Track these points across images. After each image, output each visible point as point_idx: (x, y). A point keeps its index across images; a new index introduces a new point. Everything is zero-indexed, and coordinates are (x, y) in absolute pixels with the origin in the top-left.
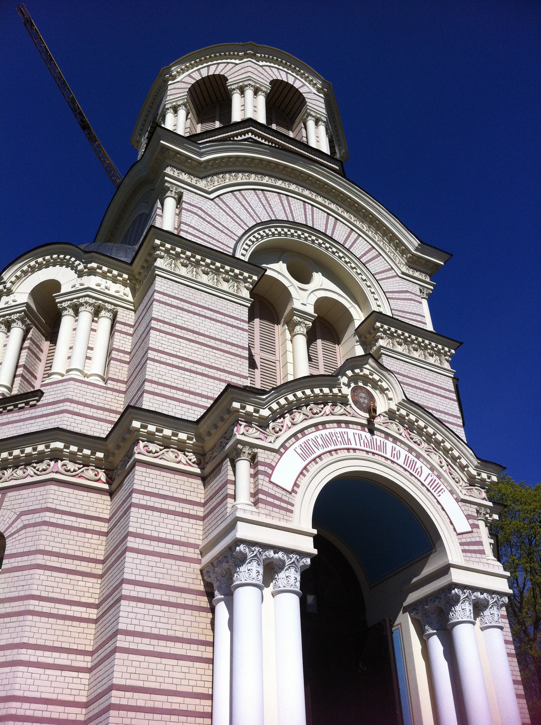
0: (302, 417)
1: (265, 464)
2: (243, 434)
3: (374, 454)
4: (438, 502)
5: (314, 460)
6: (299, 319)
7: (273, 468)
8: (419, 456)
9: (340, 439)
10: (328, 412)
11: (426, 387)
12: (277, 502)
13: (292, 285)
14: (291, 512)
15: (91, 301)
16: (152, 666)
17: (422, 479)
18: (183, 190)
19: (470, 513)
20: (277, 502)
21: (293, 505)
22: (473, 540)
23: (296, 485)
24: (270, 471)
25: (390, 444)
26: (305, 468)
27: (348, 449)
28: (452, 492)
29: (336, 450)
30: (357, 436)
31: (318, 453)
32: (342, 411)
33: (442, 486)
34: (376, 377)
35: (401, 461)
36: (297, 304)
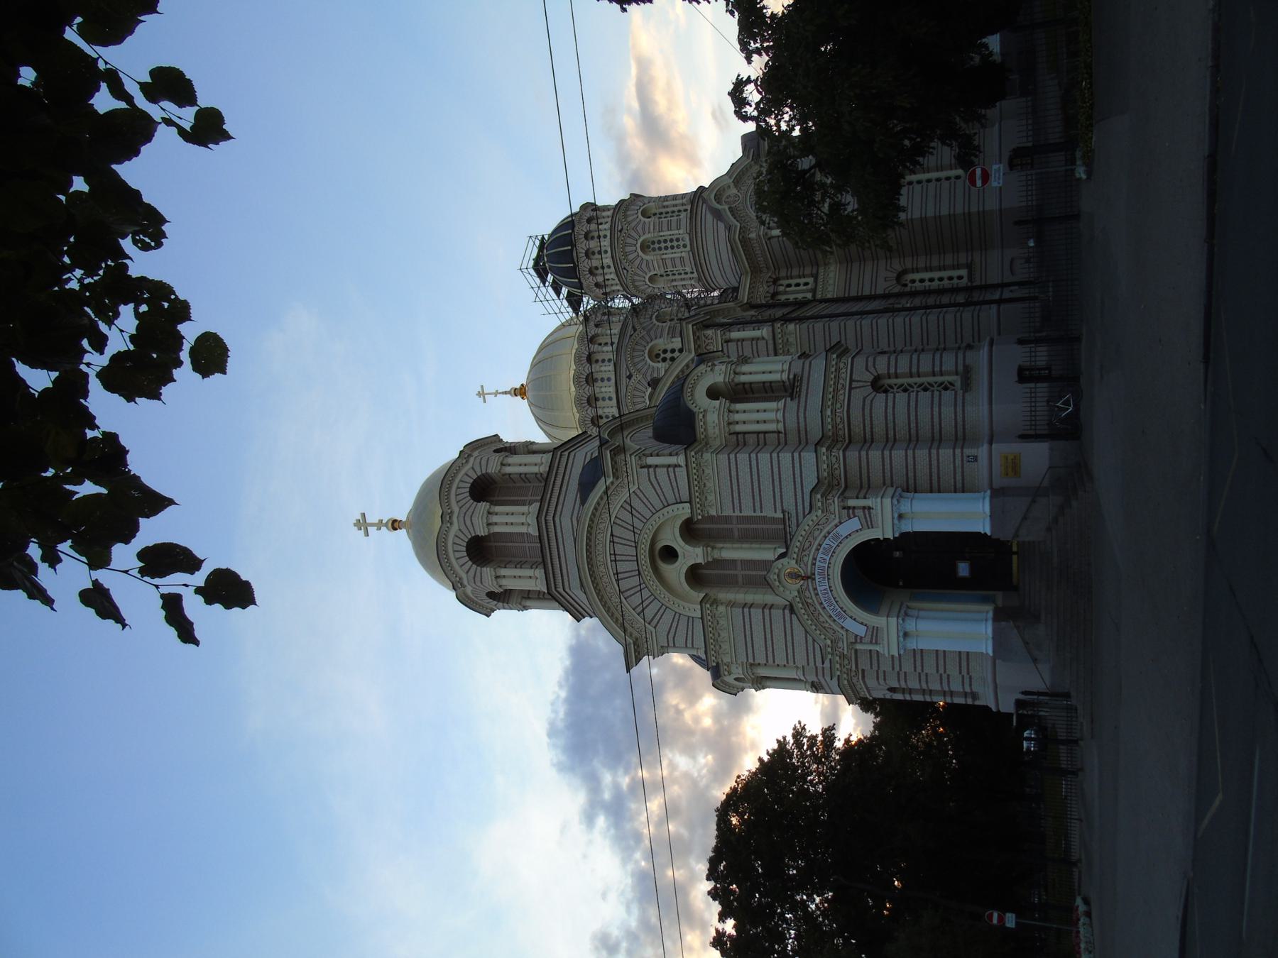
1: (856, 640)
2: (843, 649)
3: (828, 575)
4: (847, 537)
5: (844, 612)
7: (856, 636)
8: (820, 545)
9: (826, 595)
10: (811, 601)
11: (734, 481)
12: (875, 634)
18: (659, 647)
20: (875, 634)
21: (874, 627)
22: (863, 517)
23: (862, 624)
24: (859, 637)
25: (818, 564)
26: (851, 617)
27: (831, 591)
28: (837, 526)
29: (834, 598)
31: (839, 610)
32: (808, 592)
34: (777, 571)
36: (700, 560)
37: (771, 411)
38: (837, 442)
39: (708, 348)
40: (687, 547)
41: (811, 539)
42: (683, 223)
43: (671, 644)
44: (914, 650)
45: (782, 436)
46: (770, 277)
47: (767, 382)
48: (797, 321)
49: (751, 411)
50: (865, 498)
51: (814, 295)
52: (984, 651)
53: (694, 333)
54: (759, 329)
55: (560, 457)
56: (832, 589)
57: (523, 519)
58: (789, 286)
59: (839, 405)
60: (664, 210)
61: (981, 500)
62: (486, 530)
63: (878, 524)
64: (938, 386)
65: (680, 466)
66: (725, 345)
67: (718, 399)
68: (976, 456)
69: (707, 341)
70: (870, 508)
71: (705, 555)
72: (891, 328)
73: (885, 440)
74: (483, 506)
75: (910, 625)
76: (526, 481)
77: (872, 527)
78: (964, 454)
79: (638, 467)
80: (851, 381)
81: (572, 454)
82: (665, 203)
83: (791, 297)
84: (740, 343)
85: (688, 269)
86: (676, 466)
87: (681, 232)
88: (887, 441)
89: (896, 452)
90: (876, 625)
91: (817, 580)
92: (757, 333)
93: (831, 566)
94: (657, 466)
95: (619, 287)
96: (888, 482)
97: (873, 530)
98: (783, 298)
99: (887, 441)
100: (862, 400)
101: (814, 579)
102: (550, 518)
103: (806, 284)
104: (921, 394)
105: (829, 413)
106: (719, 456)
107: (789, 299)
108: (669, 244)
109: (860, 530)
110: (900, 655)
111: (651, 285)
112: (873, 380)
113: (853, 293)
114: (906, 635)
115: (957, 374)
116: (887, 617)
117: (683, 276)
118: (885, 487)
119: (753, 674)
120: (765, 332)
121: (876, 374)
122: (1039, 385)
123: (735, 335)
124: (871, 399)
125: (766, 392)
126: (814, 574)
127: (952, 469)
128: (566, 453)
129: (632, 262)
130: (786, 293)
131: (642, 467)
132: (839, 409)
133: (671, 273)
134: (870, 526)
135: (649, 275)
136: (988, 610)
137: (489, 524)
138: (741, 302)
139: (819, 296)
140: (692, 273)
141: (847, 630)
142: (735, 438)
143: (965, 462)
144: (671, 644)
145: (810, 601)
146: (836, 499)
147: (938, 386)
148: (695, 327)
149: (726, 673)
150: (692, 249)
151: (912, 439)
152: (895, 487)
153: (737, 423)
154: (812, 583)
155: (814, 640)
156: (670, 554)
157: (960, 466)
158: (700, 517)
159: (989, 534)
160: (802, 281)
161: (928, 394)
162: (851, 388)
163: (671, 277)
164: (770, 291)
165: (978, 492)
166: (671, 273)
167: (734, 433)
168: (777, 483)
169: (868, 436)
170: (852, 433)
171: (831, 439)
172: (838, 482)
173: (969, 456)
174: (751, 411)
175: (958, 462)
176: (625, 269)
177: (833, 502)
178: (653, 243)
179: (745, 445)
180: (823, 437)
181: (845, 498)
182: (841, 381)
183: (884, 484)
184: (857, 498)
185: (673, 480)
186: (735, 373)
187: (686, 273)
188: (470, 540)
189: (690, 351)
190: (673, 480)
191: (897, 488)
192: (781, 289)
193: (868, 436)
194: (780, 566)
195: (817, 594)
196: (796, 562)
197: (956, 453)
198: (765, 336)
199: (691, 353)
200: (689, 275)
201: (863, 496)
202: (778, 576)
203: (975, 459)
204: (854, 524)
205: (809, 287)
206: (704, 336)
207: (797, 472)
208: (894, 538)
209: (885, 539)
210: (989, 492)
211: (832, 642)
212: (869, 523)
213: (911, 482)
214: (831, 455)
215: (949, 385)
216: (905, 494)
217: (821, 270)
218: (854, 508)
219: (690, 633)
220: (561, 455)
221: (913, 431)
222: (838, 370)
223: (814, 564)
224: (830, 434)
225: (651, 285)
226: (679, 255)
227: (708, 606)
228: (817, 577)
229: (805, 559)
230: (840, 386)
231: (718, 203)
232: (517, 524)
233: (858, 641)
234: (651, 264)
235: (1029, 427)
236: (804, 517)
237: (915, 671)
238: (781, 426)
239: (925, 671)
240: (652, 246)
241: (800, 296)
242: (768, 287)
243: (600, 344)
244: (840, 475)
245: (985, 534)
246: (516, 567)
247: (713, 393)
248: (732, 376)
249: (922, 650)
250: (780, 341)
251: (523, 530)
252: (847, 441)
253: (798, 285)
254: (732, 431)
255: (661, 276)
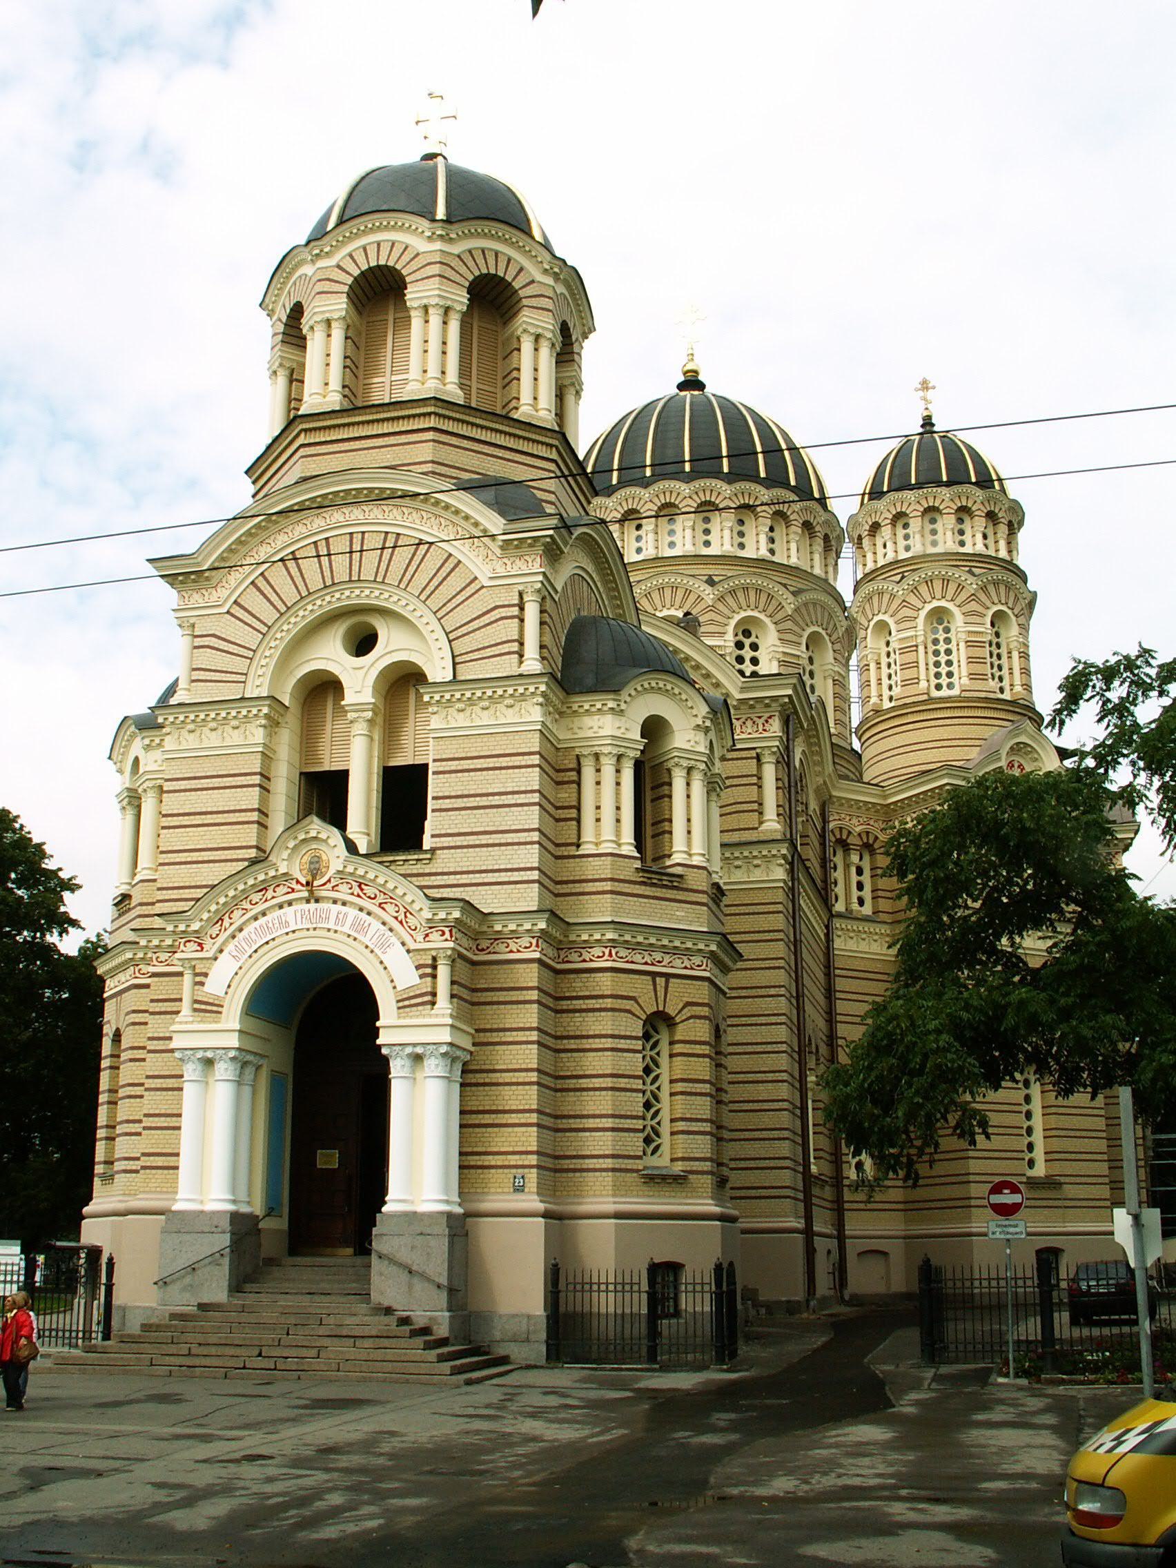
0: (241, 912)
4: (381, 962)
6: (354, 715)
7: (206, 975)
13: (345, 669)
14: (220, 1013)
15: (149, 784)
16: (167, 1137)
17: (366, 941)
19: (421, 962)
20: (209, 1008)
21: (222, 1006)
27: (287, 934)
28: (403, 944)
30: (299, 915)
33: (394, 940)
34: (323, 836)
35: (346, 929)
36: (350, 698)
37: (618, 833)
38: (558, 949)
39: (749, 723)
40: (374, 673)
41: (381, 898)
42: (979, 685)
43: (198, 642)
44: (182, 1076)
45: (572, 851)
46: (876, 838)
47: (671, 827)
48: (790, 884)
49: (618, 794)
50: (452, 996)
51: (840, 915)
52: (178, 1197)
53: (774, 699)
54: (778, 815)
55: (547, 445)
56: (291, 934)
57: (433, 371)
58: (860, 871)
59: (623, 953)
60: (1004, 651)
61: (445, 1198)
62: (415, 304)
63: (404, 1018)
64: (652, 1128)
65: (521, 663)
66: (753, 754)
67: (642, 737)
68: (523, 1191)
69: (760, 722)
70: (433, 1003)
71: (359, 708)
72: (769, 1048)
73: (559, 1034)
74: (461, 299)
75: (224, 1070)
76: (507, 380)
77: (399, 1008)
78: (526, 1170)
79: (521, 588)
80: (668, 976)
81: (552, 466)
82: (1015, 655)
83: (839, 875)
84: (754, 780)
85: (896, 691)
86: (521, 656)
87: (965, 680)
88: (556, 1038)
89: (536, 1051)
90: (224, 1010)
91: (306, 906)
92: (771, 811)
93: (331, 934)
94: (522, 620)
95: (870, 566)
96: (483, 1037)
97: (395, 1009)
98: (838, 859)
99: (556, 1038)
100: (631, 994)
101: (308, 901)
102: (432, 421)
103: (861, 902)
104: (640, 1099)
105: (610, 936)
106: (537, 735)
107: (835, 870)
108: (943, 658)
109: (395, 987)
110: (172, 1051)
111: (872, 623)
112: (667, 1014)
113: (840, 984)
114: (209, 1063)
115: (672, 1160)
116: (240, 1031)
117: (885, 682)
118: (473, 1032)
119: (145, 791)
120: (772, 824)
121: (678, 1020)
122: (644, 1297)
123: (769, 772)
124: (633, 1010)
125: (653, 824)
126: (317, 901)
127: (503, 1149)
128: (554, 456)
129: (915, 590)
130: (847, 866)
131: (521, 595)
132: (617, 953)
133: (892, 661)
134: (401, 1004)
135: (891, 621)
136: (257, 1207)
137: (426, 308)
138: (834, 786)
139: (837, 923)
140: (891, 699)
141: (216, 959)
142: (571, 766)
143: (514, 1171)
144: (198, 642)
145: (270, 894)
146: (451, 944)
147: (652, 1128)
148: (787, 700)
149: (147, 741)
150: (931, 700)
151: (559, 1081)
152: (472, 1049)
153: (598, 771)
154: (301, 899)
155: (198, 900)
156: (363, 643)
157: (506, 1163)
158: (426, 698)
159: (384, 1209)
160: (867, 893)
161: (640, 1110)
162: (654, 975)
163: (884, 660)
164: (851, 837)
165: (461, 1194)
166: (892, 661)
167: (579, 764)
168: (484, 839)
169: (565, 1004)
170: (572, 976)
171: (561, 938)
172: (483, 950)
173: (523, 1177)
174: (618, 794)
175: (513, 1160)
176: (903, 577)
177: (446, 940)
178: (947, 630)
179: (558, 783)
180: (568, 923)
181: (453, 961)
182: (667, 959)
183: (477, 1031)
184: (453, 983)
185: (496, 650)
186: (689, 770)
187: (890, 688)
188: (398, 272)
189: (743, 690)
190: (496, 650)
191: (471, 1053)
192: (855, 858)
193: (565, 1004)
194: (331, 842)
195: (281, 907)
196: (339, 872)
197: (530, 1157)
198: (765, 826)
199: (741, 692)
200: (886, 693)
201: (455, 992)
202: (315, 838)
203: (519, 1189)
204: (408, 977)
205: (855, 906)
206: (770, 717)
207: (504, 877)
208: (379, 1047)
209: (378, 1029)
210: (460, 1210)
211: (196, 932)
212: (407, 1003)
213: (480, 1078)
214: (533, 937)
215: (653, 1146)
216: (458, 1067)
217: (885, 929)
218: (434, 976)
219: (218, 676)
220: (551, 446)
221: (572, 1083)
222: (688, 953)
223: (335, 902)
224: (573, 937)
225: (872, 623)
226: (923, 676)
227: (265, 710)
228: (313, 906)
229: (344, 888)
230: (658, 956)
231: (1012, 748)
232: (424, 361)
233: (198, 979)
234: (908, 624)
235: (571, 1279)
236: (421, 888)
237: (148, 1077)
238: (586, 849)
239: (146, 1094)
240: (941, 628)
241: (839, 890)
242: (859, 835)
243: (772, 529)
244: (494, 953)
245: (384, 1203)
246: (346, 357)
247: (654, 729)
248: (685, 763)
249: (181, 1089)
250: (755, 853)
251: (414, 372)
252: (559, 967)
253: (860, 886)
254: (584, 762)
255: (888, 644)
